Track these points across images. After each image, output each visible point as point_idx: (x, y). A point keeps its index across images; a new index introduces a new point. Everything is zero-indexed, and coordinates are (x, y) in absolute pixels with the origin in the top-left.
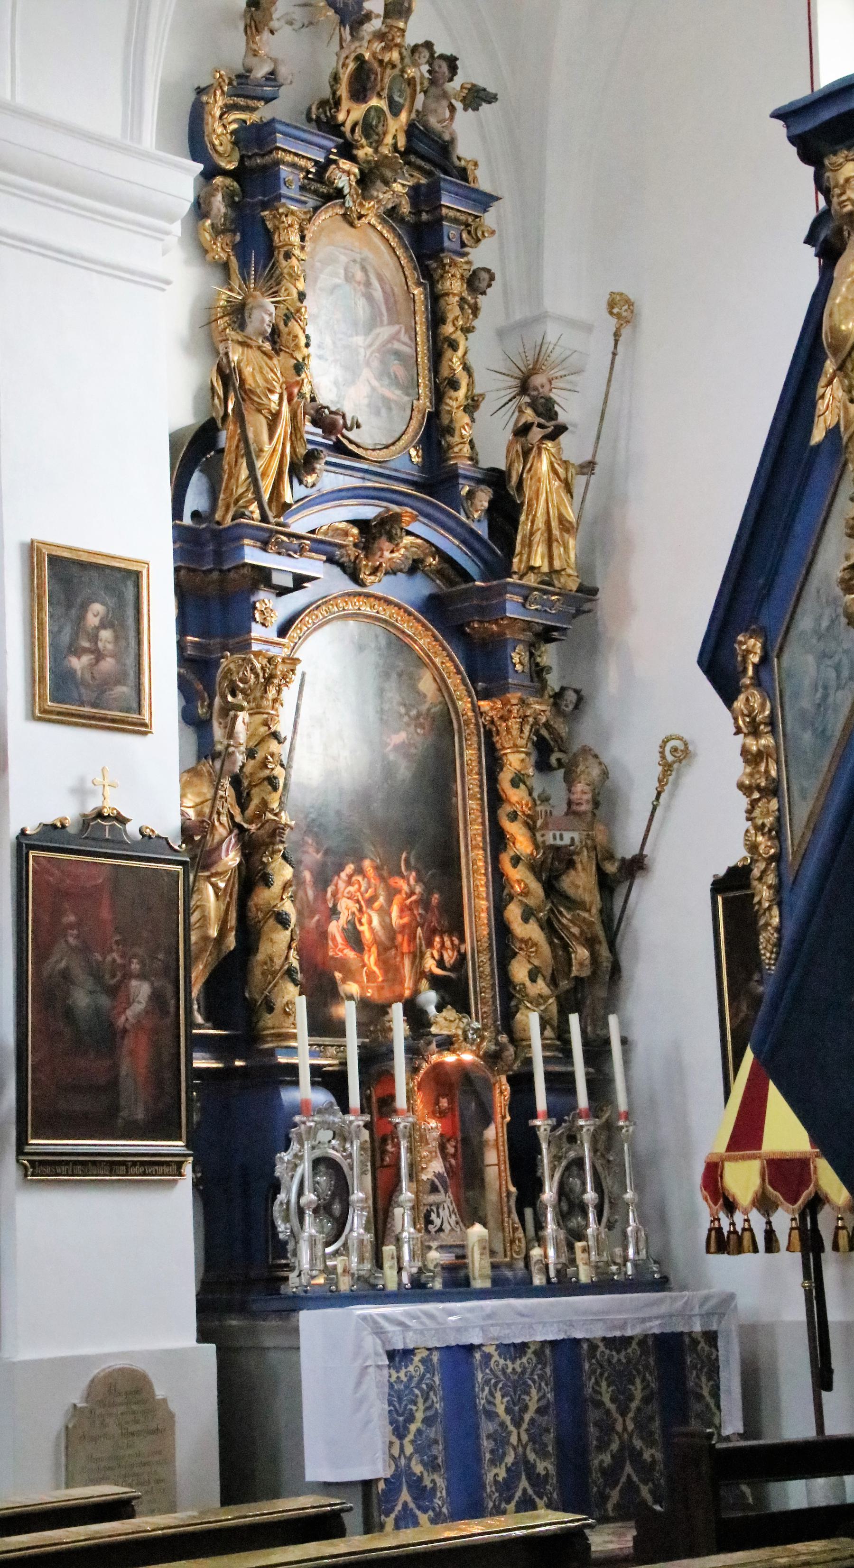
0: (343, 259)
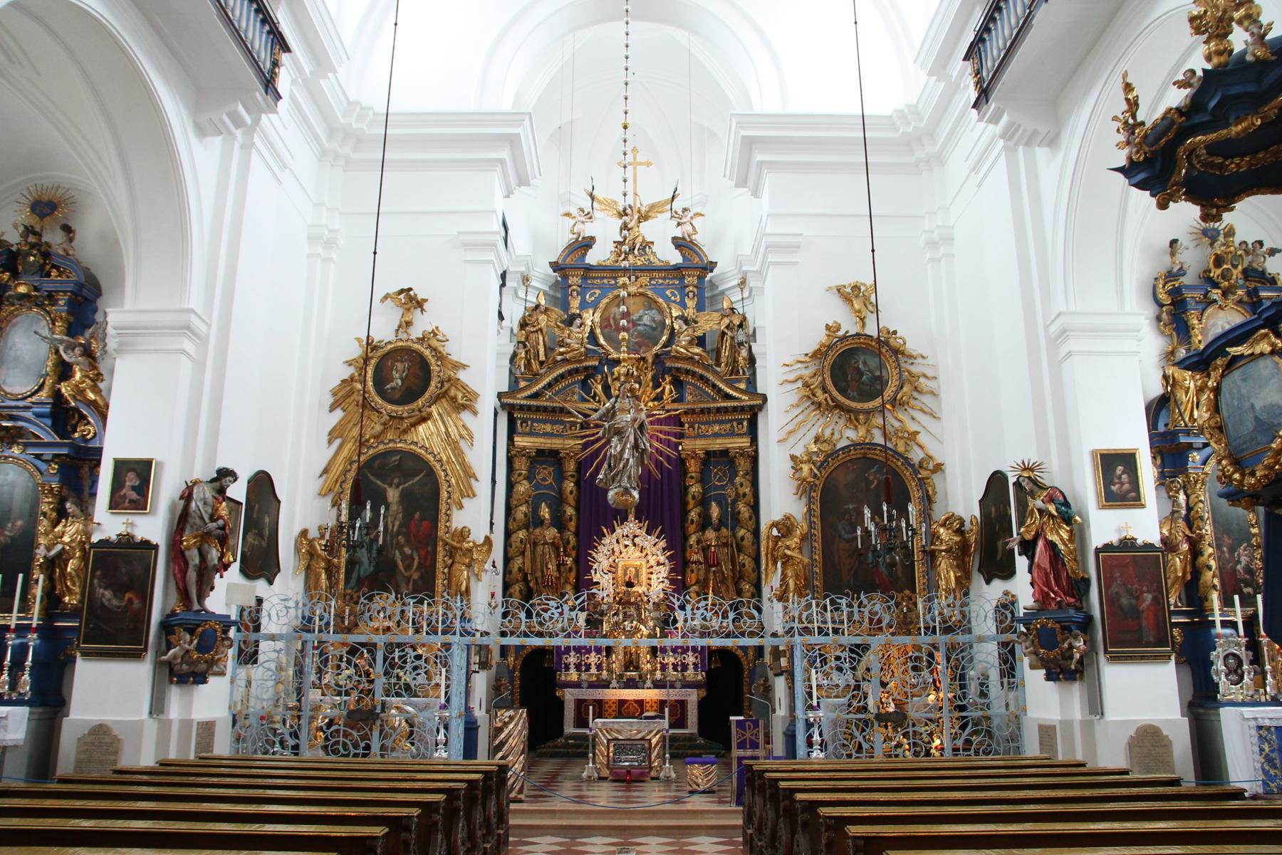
0: (1220, 323)
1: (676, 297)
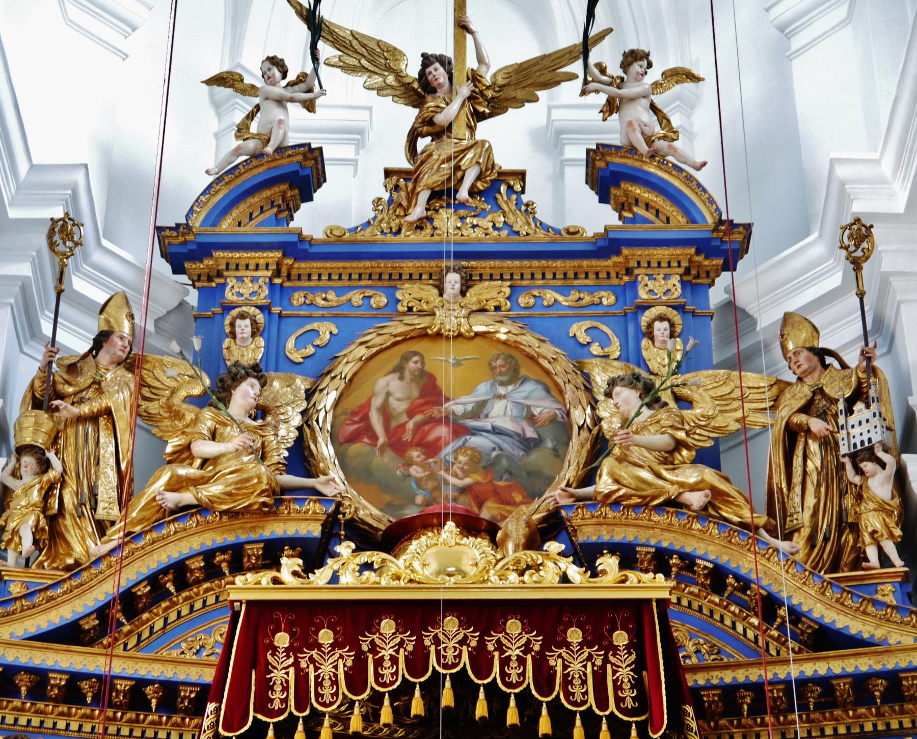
1: (605, 342)
